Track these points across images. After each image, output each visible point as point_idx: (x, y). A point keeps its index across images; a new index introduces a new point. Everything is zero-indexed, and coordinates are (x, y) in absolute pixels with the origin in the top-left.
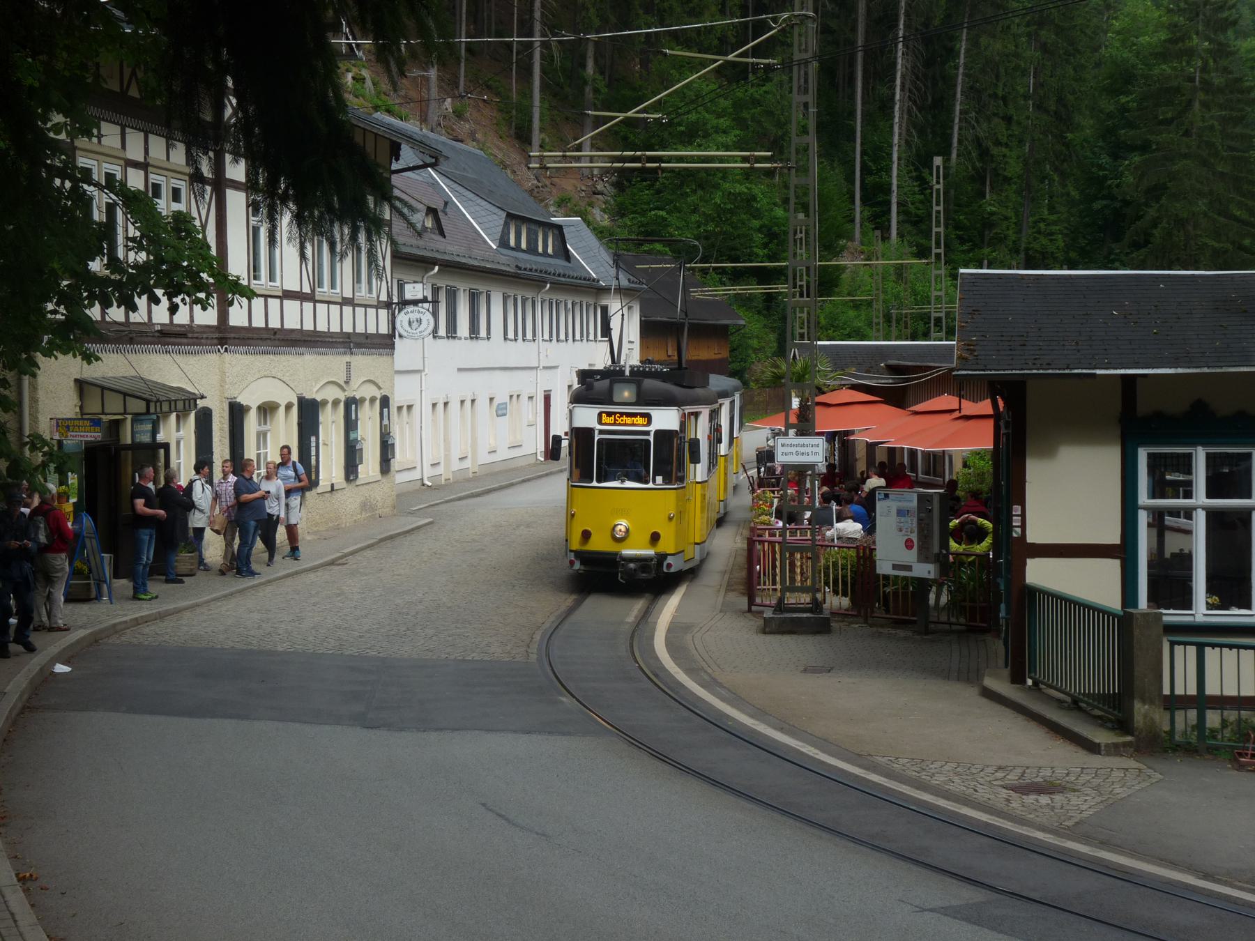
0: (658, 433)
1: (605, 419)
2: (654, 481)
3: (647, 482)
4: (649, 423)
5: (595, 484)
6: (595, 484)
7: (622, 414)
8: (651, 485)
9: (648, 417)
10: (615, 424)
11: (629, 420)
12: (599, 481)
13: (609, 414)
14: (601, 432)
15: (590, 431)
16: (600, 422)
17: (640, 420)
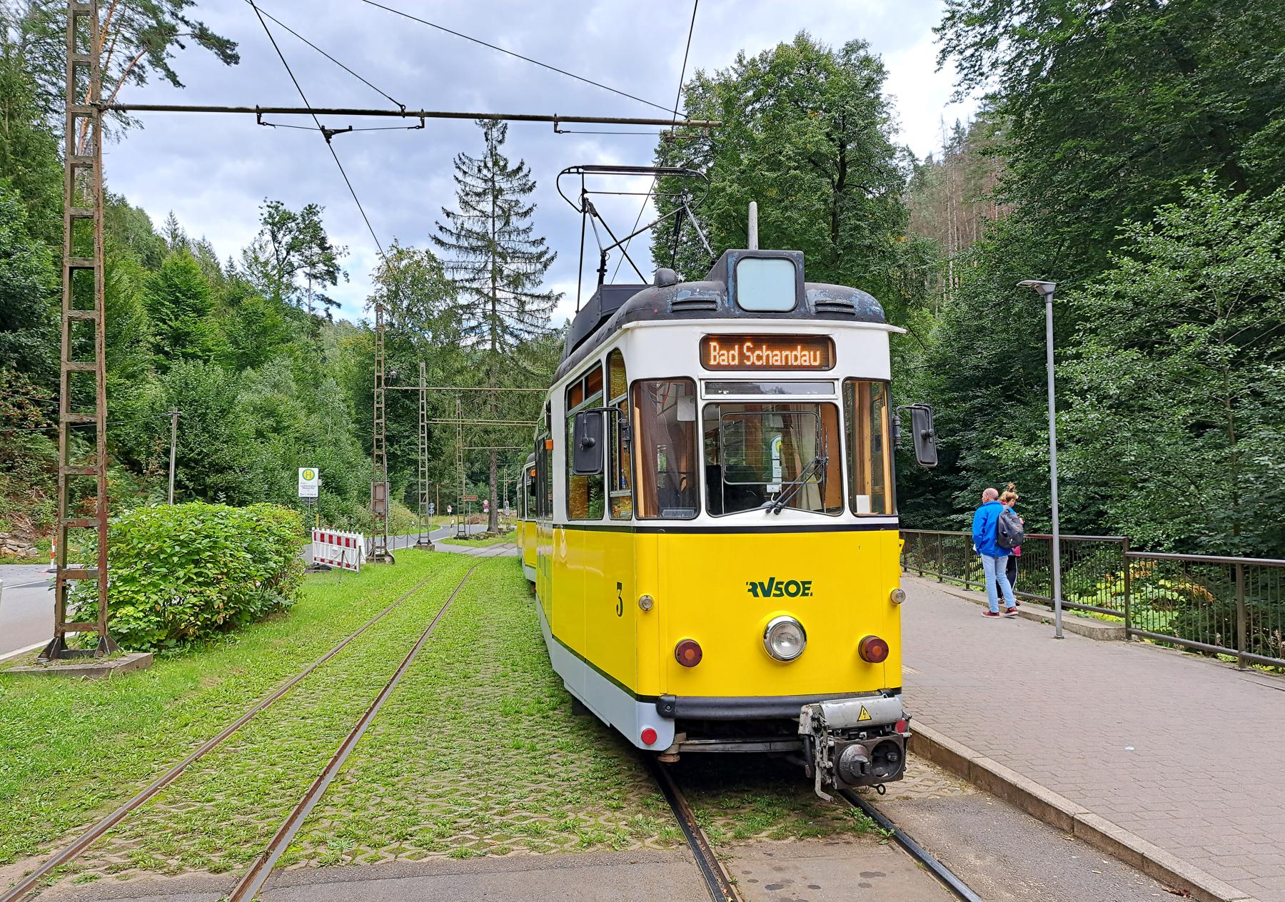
0: (852, 384)
1: (718, 354)
2: (853, 509)
3: (838, 510)
4: (828, 362)
5: (704, 519)
6: (704, 519)
7: (758, 340)
8: (846, 518)
9: (824, 343)
10: (741, 367)
11: (777, 356)
12: (714, 510)
13: (727, 341)
14: (711, 386)
15: (686, 385)
16: (705, 363)
17: (803, 355)
